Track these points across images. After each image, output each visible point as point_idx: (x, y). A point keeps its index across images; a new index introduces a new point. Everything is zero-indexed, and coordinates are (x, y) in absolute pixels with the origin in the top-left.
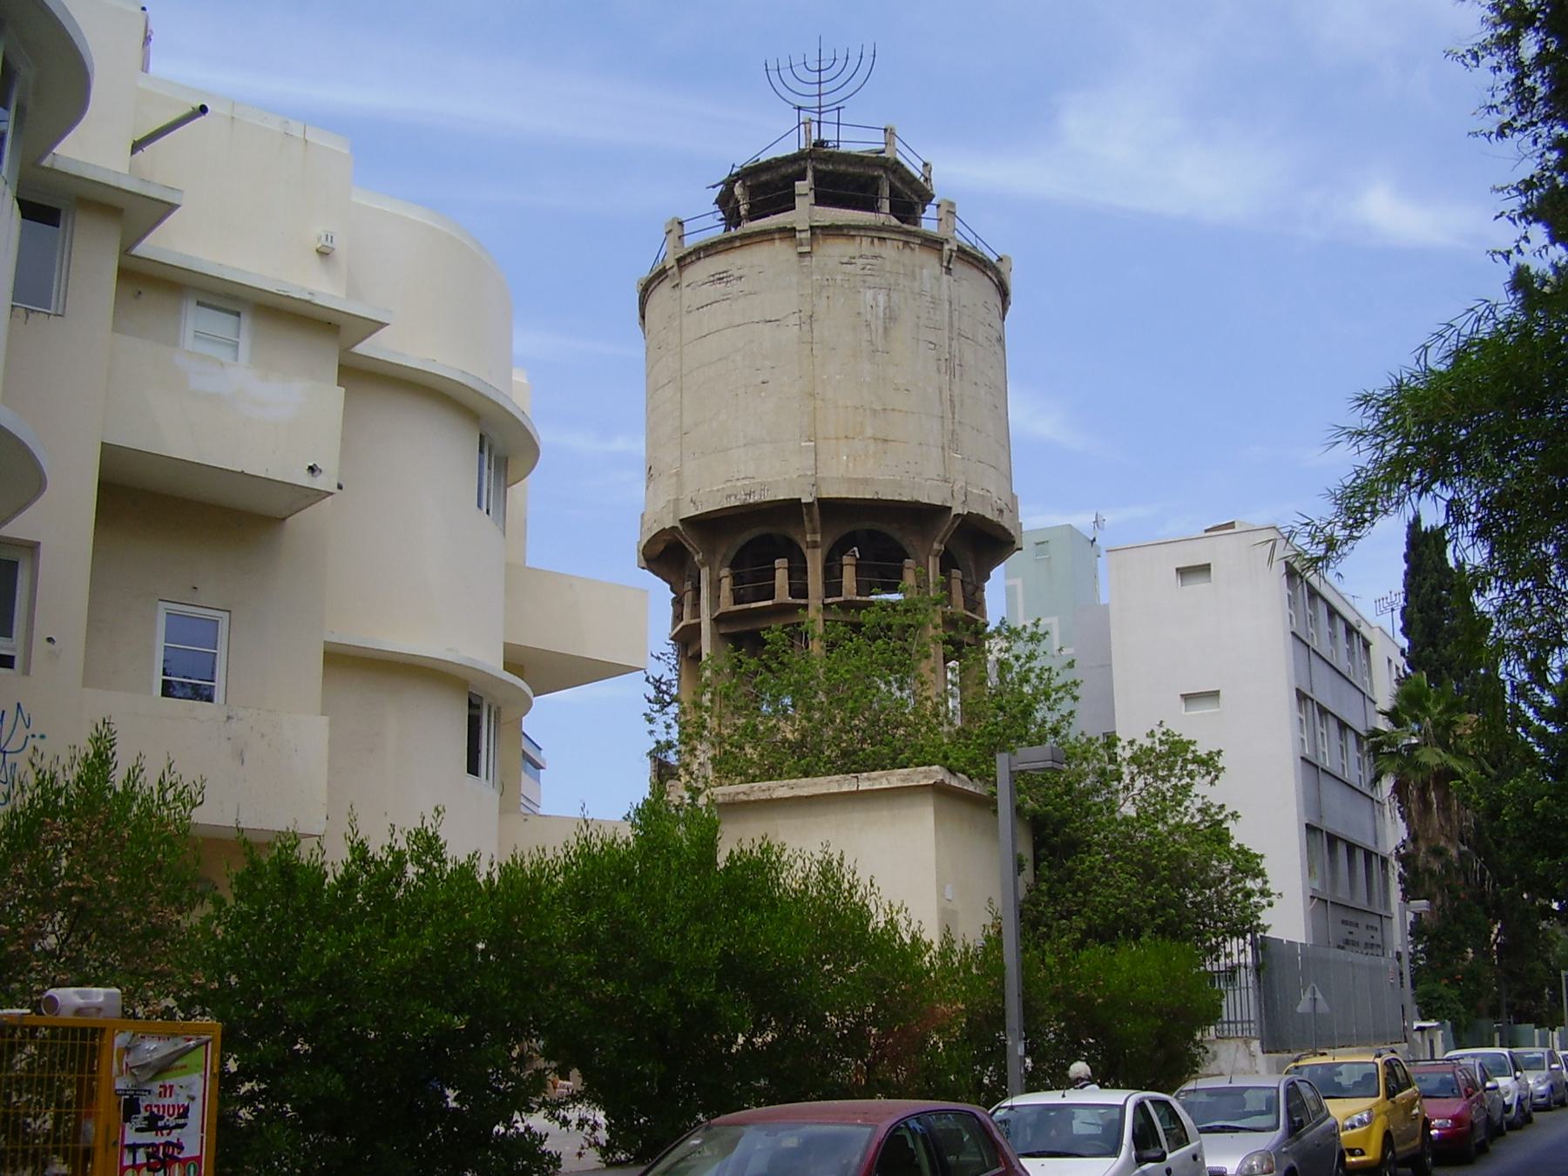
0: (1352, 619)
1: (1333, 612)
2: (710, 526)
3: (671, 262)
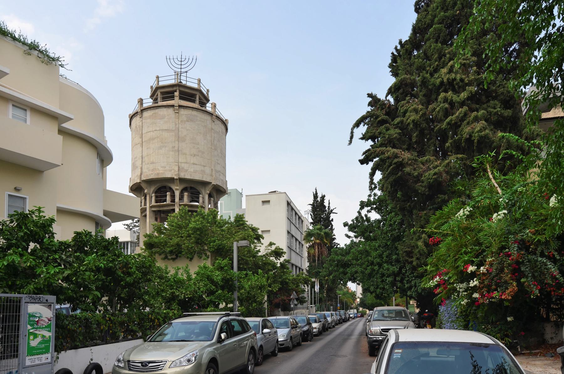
1: (296, 213)
2: (150, 182)
3: (139, 111)
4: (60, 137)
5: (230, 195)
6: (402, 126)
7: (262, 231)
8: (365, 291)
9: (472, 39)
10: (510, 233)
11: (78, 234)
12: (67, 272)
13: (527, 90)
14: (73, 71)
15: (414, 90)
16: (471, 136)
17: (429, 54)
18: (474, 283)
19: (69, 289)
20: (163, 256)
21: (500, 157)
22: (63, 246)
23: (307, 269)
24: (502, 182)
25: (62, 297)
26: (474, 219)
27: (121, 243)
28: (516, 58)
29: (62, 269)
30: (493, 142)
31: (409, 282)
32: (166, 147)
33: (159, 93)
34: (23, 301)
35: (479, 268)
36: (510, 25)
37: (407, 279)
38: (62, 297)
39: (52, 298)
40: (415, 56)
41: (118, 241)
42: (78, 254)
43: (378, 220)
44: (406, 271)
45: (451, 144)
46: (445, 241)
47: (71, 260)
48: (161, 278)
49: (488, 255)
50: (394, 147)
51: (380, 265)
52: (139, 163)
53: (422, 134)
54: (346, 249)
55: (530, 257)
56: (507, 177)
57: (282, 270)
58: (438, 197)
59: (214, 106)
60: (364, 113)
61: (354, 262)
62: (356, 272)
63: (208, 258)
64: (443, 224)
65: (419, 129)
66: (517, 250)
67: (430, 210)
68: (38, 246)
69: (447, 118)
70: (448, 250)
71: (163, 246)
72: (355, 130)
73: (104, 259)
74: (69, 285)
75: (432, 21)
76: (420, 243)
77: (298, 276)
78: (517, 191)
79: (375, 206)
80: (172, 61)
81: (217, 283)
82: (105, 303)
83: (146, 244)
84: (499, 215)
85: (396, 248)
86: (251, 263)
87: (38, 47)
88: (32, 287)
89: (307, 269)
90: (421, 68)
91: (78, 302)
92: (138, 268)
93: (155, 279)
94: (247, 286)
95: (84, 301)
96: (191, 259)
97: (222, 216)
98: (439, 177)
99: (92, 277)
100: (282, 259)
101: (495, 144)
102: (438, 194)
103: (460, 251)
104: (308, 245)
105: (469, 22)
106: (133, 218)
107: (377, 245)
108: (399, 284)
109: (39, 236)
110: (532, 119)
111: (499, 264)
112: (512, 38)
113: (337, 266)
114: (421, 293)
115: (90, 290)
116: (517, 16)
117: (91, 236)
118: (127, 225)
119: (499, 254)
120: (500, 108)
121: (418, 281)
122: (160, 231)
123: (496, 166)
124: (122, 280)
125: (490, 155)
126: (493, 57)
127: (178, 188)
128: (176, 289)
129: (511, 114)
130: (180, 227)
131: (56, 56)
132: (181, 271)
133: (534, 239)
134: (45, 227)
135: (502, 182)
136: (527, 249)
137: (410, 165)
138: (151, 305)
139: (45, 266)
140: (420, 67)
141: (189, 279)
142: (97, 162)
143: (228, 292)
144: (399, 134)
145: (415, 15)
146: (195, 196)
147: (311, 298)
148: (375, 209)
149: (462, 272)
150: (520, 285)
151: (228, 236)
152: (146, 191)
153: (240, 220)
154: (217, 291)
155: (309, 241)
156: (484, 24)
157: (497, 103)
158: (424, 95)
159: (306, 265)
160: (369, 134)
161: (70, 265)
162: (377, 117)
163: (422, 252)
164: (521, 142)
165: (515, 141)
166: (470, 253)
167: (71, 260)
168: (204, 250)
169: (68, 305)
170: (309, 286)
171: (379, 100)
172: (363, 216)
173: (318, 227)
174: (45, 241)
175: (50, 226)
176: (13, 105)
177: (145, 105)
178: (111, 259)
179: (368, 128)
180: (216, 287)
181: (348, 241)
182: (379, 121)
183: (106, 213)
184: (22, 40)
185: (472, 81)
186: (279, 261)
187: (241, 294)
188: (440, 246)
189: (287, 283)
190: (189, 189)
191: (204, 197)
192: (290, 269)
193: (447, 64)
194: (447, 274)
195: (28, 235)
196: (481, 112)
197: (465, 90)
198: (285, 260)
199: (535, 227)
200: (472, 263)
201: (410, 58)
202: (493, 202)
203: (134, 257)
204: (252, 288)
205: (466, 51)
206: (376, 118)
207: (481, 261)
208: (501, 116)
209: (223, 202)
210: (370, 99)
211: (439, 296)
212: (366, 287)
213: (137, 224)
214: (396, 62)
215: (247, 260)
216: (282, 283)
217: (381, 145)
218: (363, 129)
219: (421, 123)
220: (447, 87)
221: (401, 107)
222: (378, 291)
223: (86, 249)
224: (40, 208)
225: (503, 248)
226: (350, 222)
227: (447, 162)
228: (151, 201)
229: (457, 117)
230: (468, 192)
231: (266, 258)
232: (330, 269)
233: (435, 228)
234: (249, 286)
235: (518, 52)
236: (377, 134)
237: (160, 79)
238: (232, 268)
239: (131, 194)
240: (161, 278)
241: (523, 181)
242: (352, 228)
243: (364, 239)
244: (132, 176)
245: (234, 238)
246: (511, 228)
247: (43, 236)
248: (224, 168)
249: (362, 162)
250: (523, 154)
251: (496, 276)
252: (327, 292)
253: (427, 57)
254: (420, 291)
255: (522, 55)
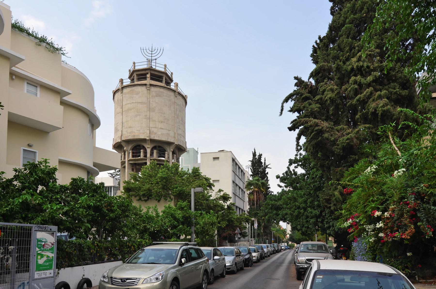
0: (242, 169)
1: (239, 168)
2: (128, 142)
3: (120, 88)
4: (62, 107)
5: (188, 153)
6: (321, 102)
7: (213, 181)
8: (293, 229)
9: (376, 36)
10: (408, 186)
11: (74, 180)
12: (66, 209)
13: (420, 75)
14: (72, 58)
15: (330, 74)
16: (376, 110)
17: (342, 47)
18: (380, 225)
19: (67, 221)
20: (138, 198)
21: (400, 127)
22: (63, 188)
23: (248, 210)
24: (401, 146)
25: (62, 227)
26: (379, 175)
27: (106, 187)
28: (411, 50)
29: (62, 206)
30: (394, 115)
31: (327, 223)
32: (140, 115)
33: (135, 75)
34: (33, 230)
35: (383, 213)
36: (405, 25)
37: (326, 220)
38: (62, 227)
39: (55, 228)
40: (331, 48)
41: (104, 186)
42: (74, 195)
43: (303, 174)
44: (326, 214)
45: (360, 116)
46: (356, 191)
47: (69, 199)
48: (136, 214)
49: (390, 203)
50: (315, 118)
51: (305, 209)
52: (120, 128)
53: (337, 108)
54: (278, 196)
55: (424, 205)
56: (405, 143)
57: (228, 211)
58: (350, 157)
59: (177, 85)
60: (291, 91)
61: (285, 206)
62: (286, 214)
63: (172, 200)
64: (354, 178)
65: (334, 104)
66: (414, 200)
67: (344, 167)
68: (45, 188)
69: (356, 96)
70: (359, 198)
71: (138, 190)
72: (285, 104)
73: (93, 199)
74: (67, 218)
75: (344, 21)
76: (336, 193)
77: (241, 216)
78: (413, 154)
79: (300, 163)
80: (145, 51)
81: (179, 219)
82: (94, 232)
83: (125, 188)
84: (399, 172)
85: (318, 196)
86: (205, 205)
87: (46, 40)
88: (40, 219)
89: (248, 210)
90: (336, 58)
91: (74, 231)
92: (119, 207)
93: (131, 215)
94: (201, 223)
95: (78, 231)
96: (159, 201)
97: (182, 168)
98: (350, 142)
99: (84, 212)
100: (228, 203)
101: (395, 117)
102: (350, 154)
103: (368, 199)
104: (248, 192)
105: (373, 23)
106: (115, 169)
107: (302, 193)
108: (320, 225)
109: (46, 180)
110: (424, 98)
111: (400, 210)
112: (407, 35)
113: (271, 209)
114: (338, 232)
115: (83, 222)
116: (410, 18)
117: (84, 181)
118: (111, 174)
119: (400, 203)
120: (399, 89)
121: (335, 222)
122: (135, 179)
123: (396, 134)
124: (107, 216)
125: (391, 125)
126: (392, 49)
127: (149, 146)
128: (148, 224)
129: (407, 94)
130: (151, 176)
131: (59, 47)
132: (151, 210)
133: (428, 192)
134: (50, 174)
135: (401, 146)
136: (422, 199)
137: (328, 132)
138: (129, 235)
139: (50, 204)
140: (335, 57)
141: (158, 216)
142: (89, 126)
143: (187, 227)
144: (319, 108)
145: (331, 17)
146: (162, 153)
147: (251, 233)
148: (301, 166)
149: (370, 216)
150: (417, 227)
151: (187, 184)
152: (125, 148)
153: (196, 172)
154: (178, 226)
155: (249, 189)
156: (385, 24)
157: (396, 85)
158: (338, 79)
159: (247, 207)
160: (296, 108)
161: (68, 203)
162: (302, 95)
163: (338, 200)
164: (416, 116)
165: (411, 114)
166: (377, 201)
167: (69, 199)
168: (169, 194)
169: (66, 234)
170: (250, 224)
171: (303, 82)
172: (291, 170)
173: (257, 178)
174: (50, 184)
175: (54, 173)
176: (28, 83)
177: (125, 84)
178: (98, 200)
179: (295, 103)
180: (178, 222)
181: (280, 190)
182: (303, 98)
183: (95, 165)
184: (35, 35)
185: (376, 67)
186: (226, 204)
187: (197, 228)
188: (353, 195)
189: (232, 221)
190: (157, 148)
191: (169, 153)
192: (235, 211)
193: (356, 54)
194: (358, 217)
195: (37, 180)
196: (384, 92)
197: (371, 74)
198: (231, 203)
199: (428, 182)
200: (378, 209)
201: (327, 50)
202: (394, 162)
203: (116, 198)
204: (205, 224)
205: (371, 45)
206: (301, 96)
207: (385, 208)
208: (400, 95)
209: (183, 158)
210: (296, 81)
211: (352, 234)
212: (294, 226)
213: (118, 173)
214: (316, 53)
215: (201, 203)
216: (228, 221)
217: (305, 116)
218: (291, 104)
219: (336, 100)
220: (357, 72)
221: (320, 87)
222: (304, 229)
223: (80, 191)
224: (46, 160)
225: (402, 198)
226: (281, 175)
227: (357, 130)
228: (129, 156)
229: (364, 95)
230: (374, 154)
231: (216, 201)
232: (266, 211)
233: (348, 182)
234: (203, 222)
235: (413, 45)
236: (302, 107)
237: (136, 65)
238: (190, 209)
239: (114, 151)
240: (136, 214)
241: (418, 146)
242: (282, 180)
243: (292, 188)
244: (115, 137)
245: (192, 186)
246: (409, 183)
247: (49, 181)
248: (184, 132)
249: (290, 129)
250: (418, 124)
251: (398, 220)
252: (263, 229)
253: (340, 49)
254: (336, 230)
255: (416, 48)
